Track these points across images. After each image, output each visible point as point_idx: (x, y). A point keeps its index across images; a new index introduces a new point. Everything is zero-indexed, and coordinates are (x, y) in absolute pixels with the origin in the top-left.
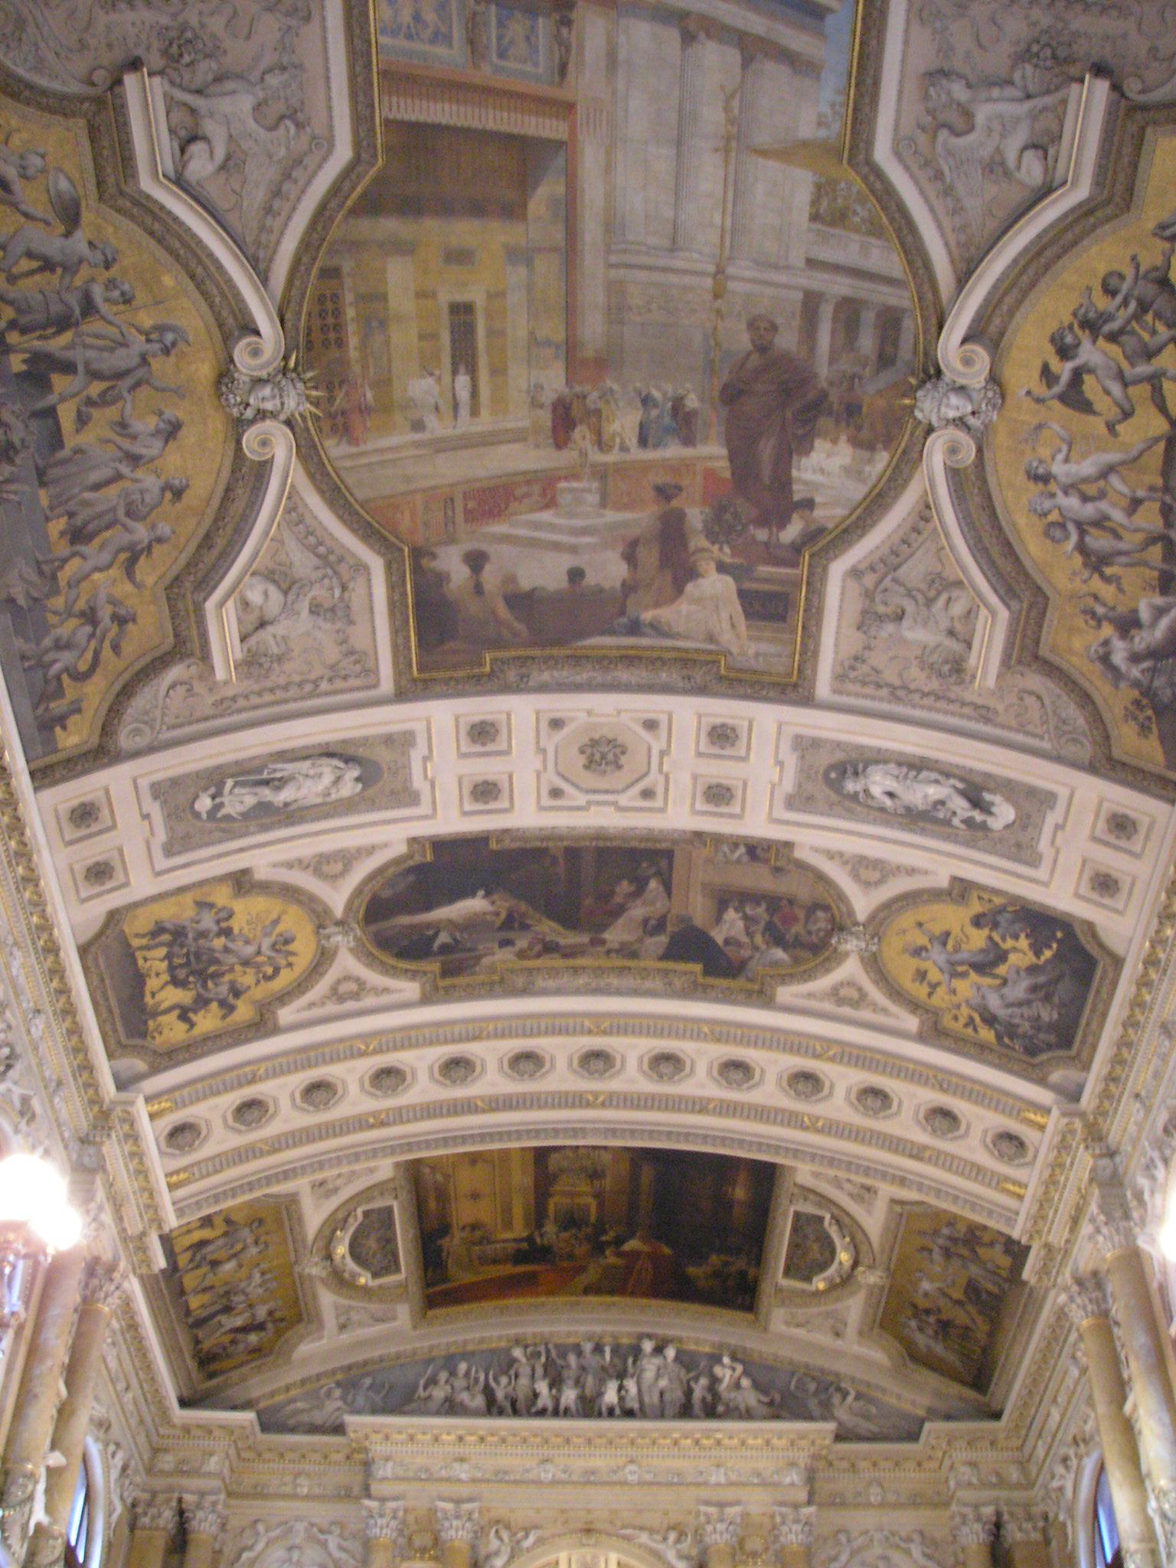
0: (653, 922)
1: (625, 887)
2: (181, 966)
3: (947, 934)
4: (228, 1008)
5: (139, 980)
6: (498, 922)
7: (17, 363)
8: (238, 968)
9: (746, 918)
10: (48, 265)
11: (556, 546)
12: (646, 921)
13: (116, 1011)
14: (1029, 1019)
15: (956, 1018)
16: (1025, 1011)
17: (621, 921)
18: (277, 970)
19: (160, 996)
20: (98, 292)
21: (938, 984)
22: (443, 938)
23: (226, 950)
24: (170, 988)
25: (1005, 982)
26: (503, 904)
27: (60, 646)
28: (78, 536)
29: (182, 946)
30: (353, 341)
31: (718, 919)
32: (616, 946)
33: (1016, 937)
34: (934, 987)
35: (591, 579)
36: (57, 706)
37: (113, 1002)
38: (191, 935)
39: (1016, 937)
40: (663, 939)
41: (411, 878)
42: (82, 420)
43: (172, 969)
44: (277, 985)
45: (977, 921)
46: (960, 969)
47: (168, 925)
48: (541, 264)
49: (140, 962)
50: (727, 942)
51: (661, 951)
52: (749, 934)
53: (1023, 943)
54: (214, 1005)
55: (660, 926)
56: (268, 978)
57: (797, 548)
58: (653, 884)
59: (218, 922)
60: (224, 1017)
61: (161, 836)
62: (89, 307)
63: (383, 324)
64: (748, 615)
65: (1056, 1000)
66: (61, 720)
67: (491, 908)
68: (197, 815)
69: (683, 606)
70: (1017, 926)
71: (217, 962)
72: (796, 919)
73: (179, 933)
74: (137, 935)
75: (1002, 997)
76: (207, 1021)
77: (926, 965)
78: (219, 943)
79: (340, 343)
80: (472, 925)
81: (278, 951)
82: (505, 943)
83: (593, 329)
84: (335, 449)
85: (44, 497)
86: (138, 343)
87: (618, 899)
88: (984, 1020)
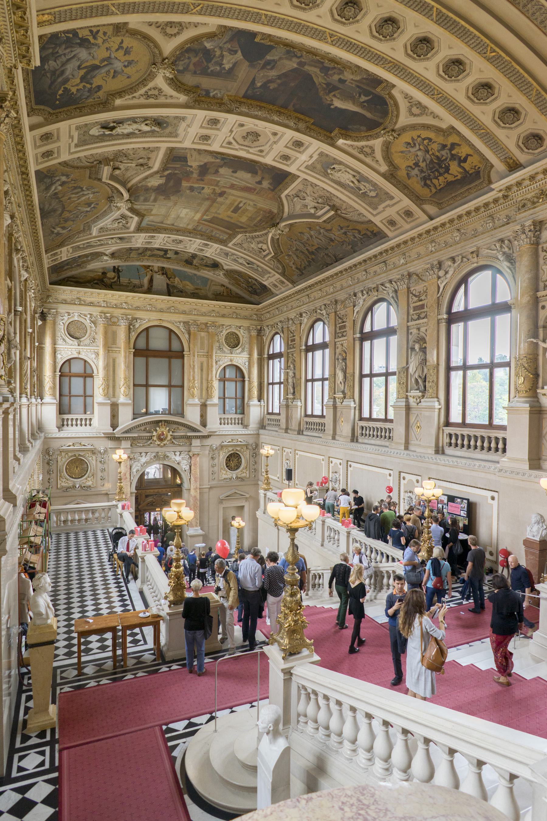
0: (268, 67)
1: (272, 86)
2: (438, 172)
3: (114, 77)
4: (453, 146)
5: (449, 184)
6: (336, 93)
7: (313, 257)
8: (430, 153)
9: (221, 65)
10: (297, 256)
11: (236, 178)
12: (272, 69)
13: (466, 188)
14: (60, 56)
15: (105, 34)
16: (64, 59)
17: (284, 71)
18: (424, 139)
19: (456, 173)
20: (294, 249)
21: (117, 50)
22: (363, 98)
23: (424, 160)
24: (450, 172)
25: (79, 67)
26: (327, 99)
27: (355, 237)
28: (332, 240)
29: (429, 175)
30: (259, 219)
31: (235, 64)
32: (294, 59)
33: (78, 90)
34: (120, 47)
35: (231, 170)
36: (369, 234)
37: (462, 190)
38: (424, 175)
39: (78, 90)
40: (268, 57)
41: (350, 127)
42: (313, 246)
43: (441, 175)
44: (432, 135)
45: (99, 88)
46: (106, 63)
47: (423, 183)
48: (214, 211)
49: (441, 186)
50: (236, 52)
51: (274, 50)
52: (222, 56)
53: (74, 90)
54: (453, 152)
55: (268, 63)
56: (430, 140)
57: (167, 170)
58: (259, 85)
59: (413, 169)
60: (459, 145)
61: (388, 202)
62: (297, 250)
63: (251, 217)
64: (186, 158)
65: (49, 75)
66: (372, 232)
67: (334, 99)
68: (377, 194)
69: (206, 161)
70: (79, 94)
71: (432, 161)
72: (194, 64)
73: (424, 179)
74: (431, 191)
75: (79, 59)
76: (463, 151)
77: (123, 59)
78: (423, 165)
79: (261, 220)
80: (348, 97)
81: (415, 144)
82: (341, 81)
83: (207, 203)
84: (275, 211)
85: (330, 247)
86: (294, 242)
87: (279, 81)
88: (87, 40)
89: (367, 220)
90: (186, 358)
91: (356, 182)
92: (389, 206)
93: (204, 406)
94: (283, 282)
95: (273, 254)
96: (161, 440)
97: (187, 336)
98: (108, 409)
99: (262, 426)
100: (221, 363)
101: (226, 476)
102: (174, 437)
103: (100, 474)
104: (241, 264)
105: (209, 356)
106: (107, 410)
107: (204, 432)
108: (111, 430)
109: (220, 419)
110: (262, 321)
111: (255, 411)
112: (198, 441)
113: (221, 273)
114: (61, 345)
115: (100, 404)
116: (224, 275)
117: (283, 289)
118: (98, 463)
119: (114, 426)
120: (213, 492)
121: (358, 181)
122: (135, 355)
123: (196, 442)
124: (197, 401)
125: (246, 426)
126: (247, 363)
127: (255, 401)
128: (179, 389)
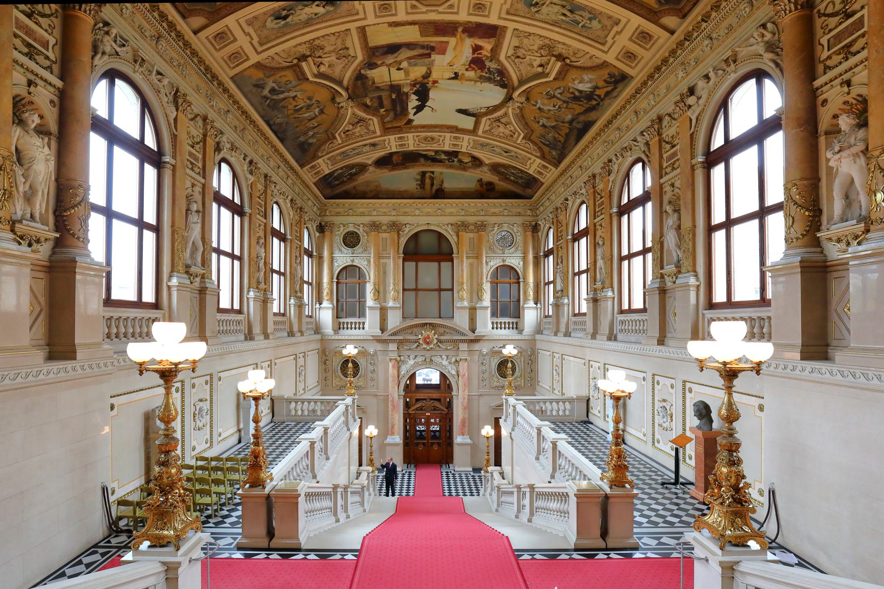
89: (600, 62)
90: (455, 261)
91: (568, 14)
92: (618, 33)
93: (473, 310)
94: (545, 167)
95: (522, 135)
96: (428, 343)
97: (455, 238)
98: (378, 312)
99: (539, 330)
100: (492, 263)
101: (498, 384)
102: (439, 341)
103: (370, 375)
104: (499, 154)
105: (478, 257)
106: (377, 313)
107: (471, 336)
108: (378, 332)
109: (493, 323)
110: (537, 216)
111: (530, 315)
112: (466, 345)
113: (485, 169)
114: (337, 254)
115: (371, 308)
116: (490, 171)
117: (549, 175)
118: (369, 365)
119: (383, 330)
120: (483, 400)
121: (571, 11)
122: (404, 260)
123: (464, 347)
124: (466, 304)
125: (521, 332)
126: (521, 263)
127: (531, 304)
128: (450, 292)
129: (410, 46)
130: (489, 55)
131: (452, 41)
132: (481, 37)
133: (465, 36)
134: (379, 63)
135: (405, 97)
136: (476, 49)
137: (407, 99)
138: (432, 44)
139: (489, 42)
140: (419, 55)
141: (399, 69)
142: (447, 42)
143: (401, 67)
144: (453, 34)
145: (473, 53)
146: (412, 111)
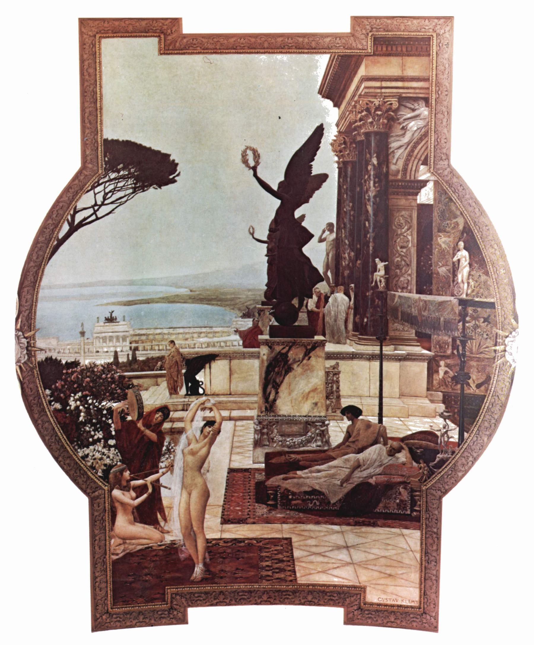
129: (318, 508)
130: (116, 493)
131: (214, 529)
132: (146, 553)
133: (188, 550)
134: (403, 457)
135: (347, 255)
136: (150, 511)
137: (337, 244)
138: (262, 510)
139: (124, 539)
140: (297, 466)
141: (353, 412)
142: (225, 521)
143: (346, 423)
144: (212, 547)
145: (157, 486)
146: (326, 162)
